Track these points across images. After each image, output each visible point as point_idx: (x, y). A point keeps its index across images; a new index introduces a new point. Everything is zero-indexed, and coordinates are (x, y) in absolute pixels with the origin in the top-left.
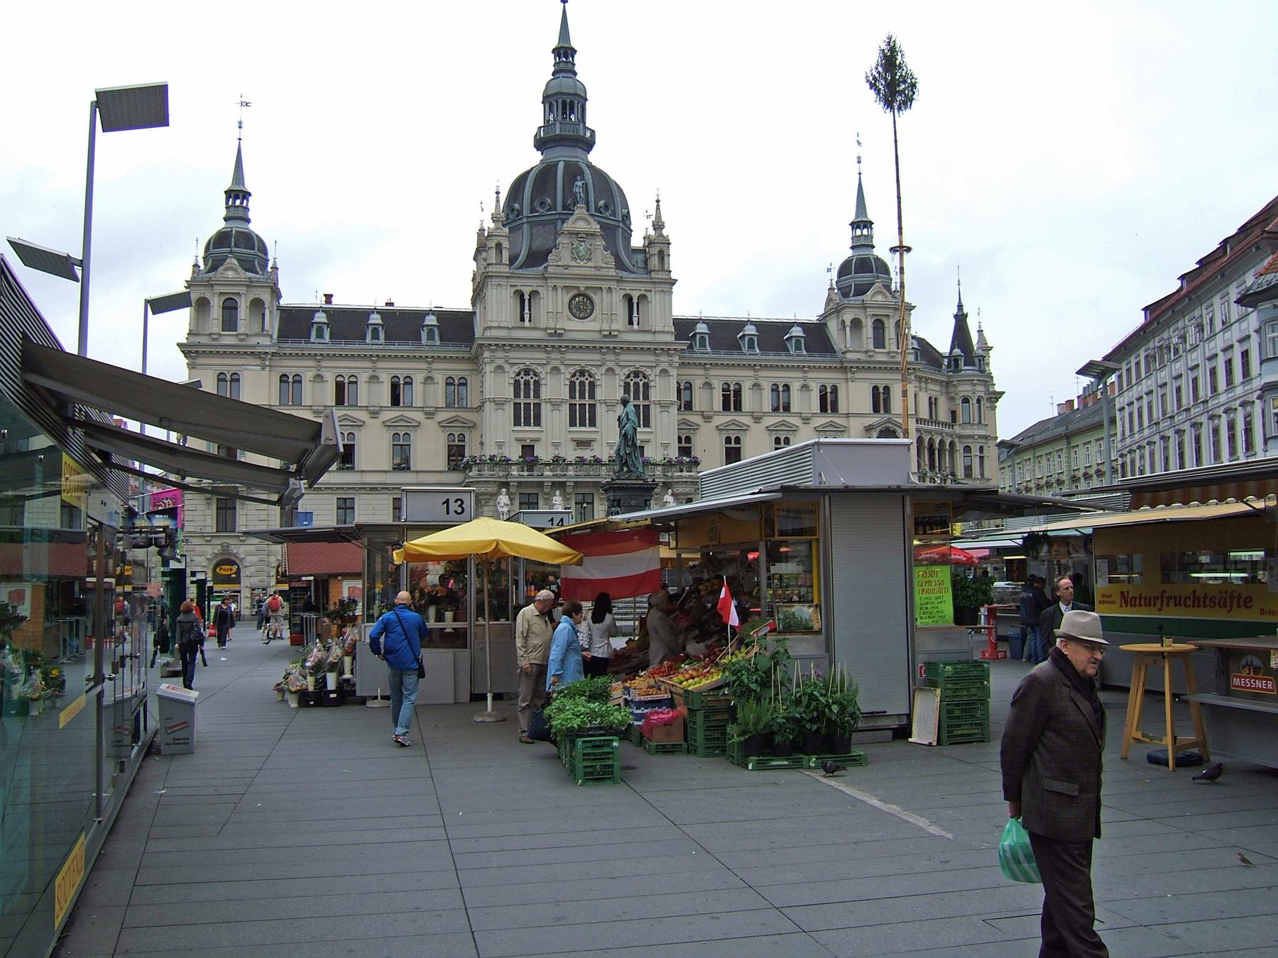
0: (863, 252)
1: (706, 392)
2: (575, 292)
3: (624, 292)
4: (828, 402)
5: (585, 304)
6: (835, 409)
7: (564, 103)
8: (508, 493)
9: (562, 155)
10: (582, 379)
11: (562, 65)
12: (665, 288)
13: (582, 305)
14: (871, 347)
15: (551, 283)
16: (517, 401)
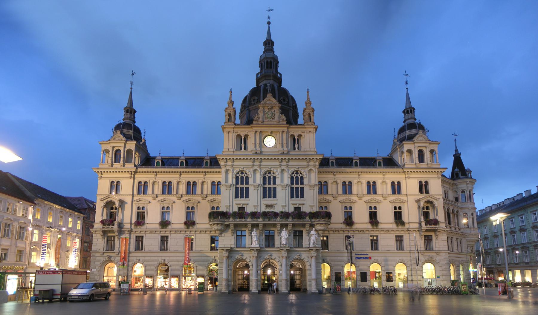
1: (334, 186)
4: (396, 188)
6: (399, 193)
7: (267, 62)
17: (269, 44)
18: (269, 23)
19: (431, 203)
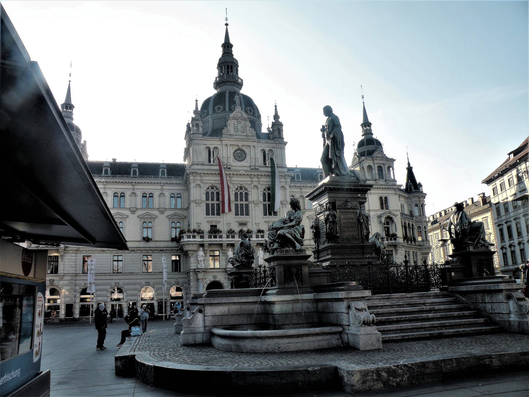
0: (369, 136)
2: (237, 148)
3: (262, 148)
5: (241, 154)
7: (228, 66)
8: (204, 250)
9: (228, 88)
10: (241, 191)
11: (226, 51)
12: (281, 145)
13: (240, 154)
14: (377, 177)
15: (224, 143)
16: (208, 202)
17: (227, 46)
18: (227, 25)
19: (391, 219)
